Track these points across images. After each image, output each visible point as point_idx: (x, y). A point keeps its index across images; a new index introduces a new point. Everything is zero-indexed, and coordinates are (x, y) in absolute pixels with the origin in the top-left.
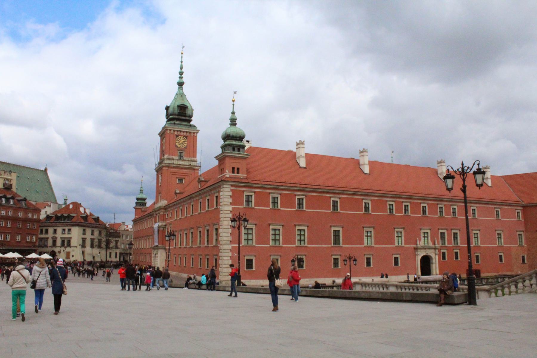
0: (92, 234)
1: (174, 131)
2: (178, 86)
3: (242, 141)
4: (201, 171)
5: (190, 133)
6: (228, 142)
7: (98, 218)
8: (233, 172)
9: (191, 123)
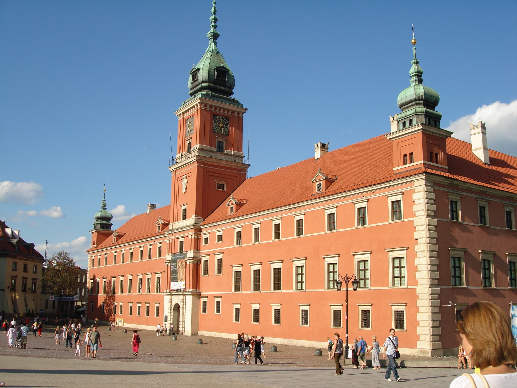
0: (25, 271)
1: (211, 107)
3: (433, 108)
4: (251, 173)
5: (233, 112)
6: (421, 109)
7: (32, 245)
8: (431, 161)
9: (232, 97)
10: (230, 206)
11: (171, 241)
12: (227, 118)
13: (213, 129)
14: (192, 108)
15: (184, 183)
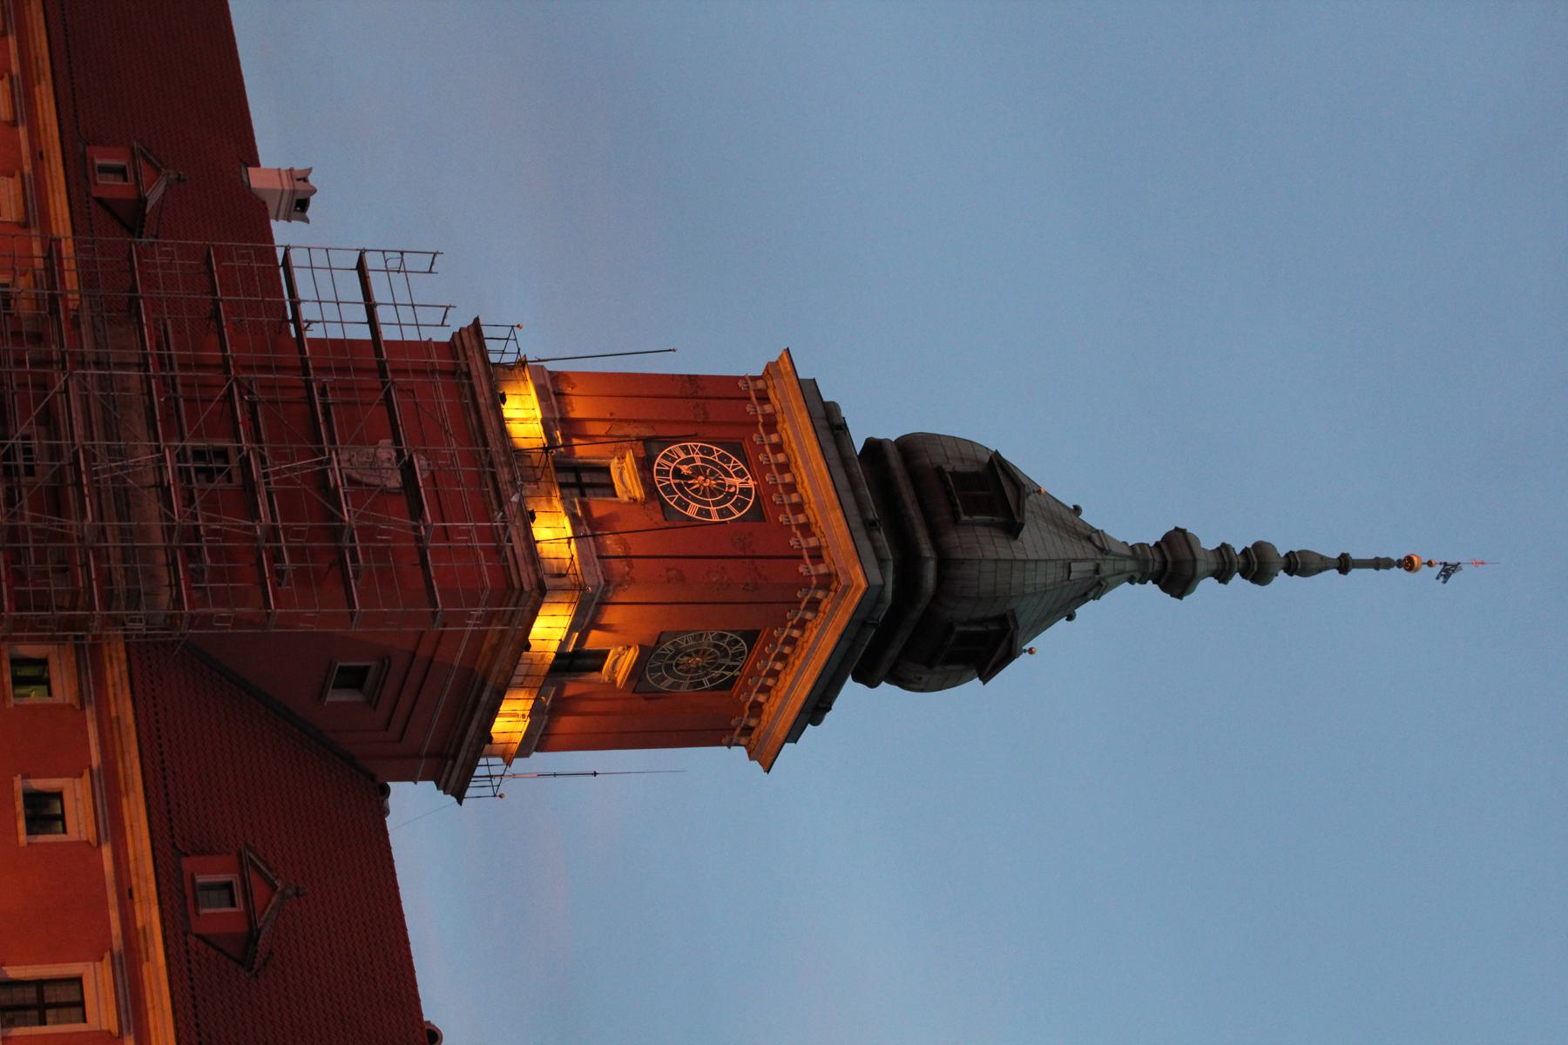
2: (1152, 537)
4: (412, 806)
10: (232, 877)
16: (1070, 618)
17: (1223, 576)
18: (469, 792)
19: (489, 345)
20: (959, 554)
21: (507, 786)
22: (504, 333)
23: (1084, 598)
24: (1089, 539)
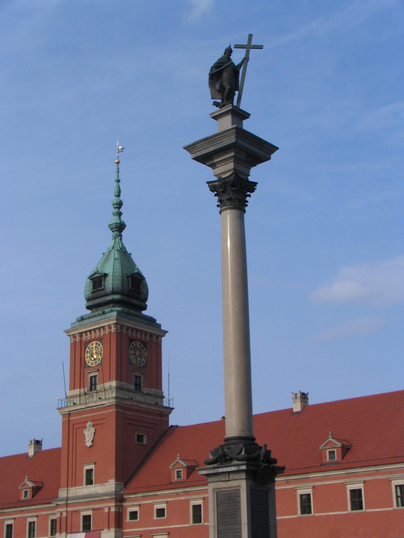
1: (128, 328)
2: (110, 234)
5: (151, 335)
9: (144, 312)
11: (64, 515)
12: (144, 344)
13: (130, 360)
14: (99, 328)
15: (89, 434)
16: (131, 254)
17: (120, 214)
18: (171, 406)
19: (63, 406)
20: (111, 289)
21: (171, 398)
22: (60, 402)
23: (125, 252)
24: (110, 251)
